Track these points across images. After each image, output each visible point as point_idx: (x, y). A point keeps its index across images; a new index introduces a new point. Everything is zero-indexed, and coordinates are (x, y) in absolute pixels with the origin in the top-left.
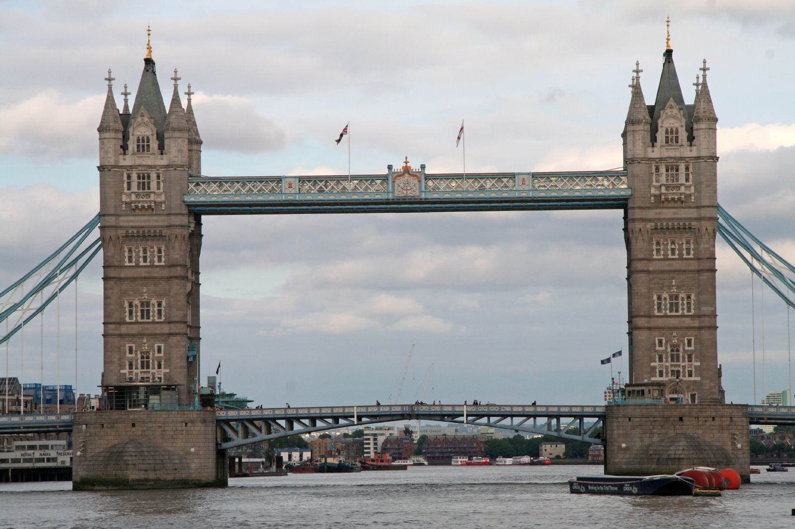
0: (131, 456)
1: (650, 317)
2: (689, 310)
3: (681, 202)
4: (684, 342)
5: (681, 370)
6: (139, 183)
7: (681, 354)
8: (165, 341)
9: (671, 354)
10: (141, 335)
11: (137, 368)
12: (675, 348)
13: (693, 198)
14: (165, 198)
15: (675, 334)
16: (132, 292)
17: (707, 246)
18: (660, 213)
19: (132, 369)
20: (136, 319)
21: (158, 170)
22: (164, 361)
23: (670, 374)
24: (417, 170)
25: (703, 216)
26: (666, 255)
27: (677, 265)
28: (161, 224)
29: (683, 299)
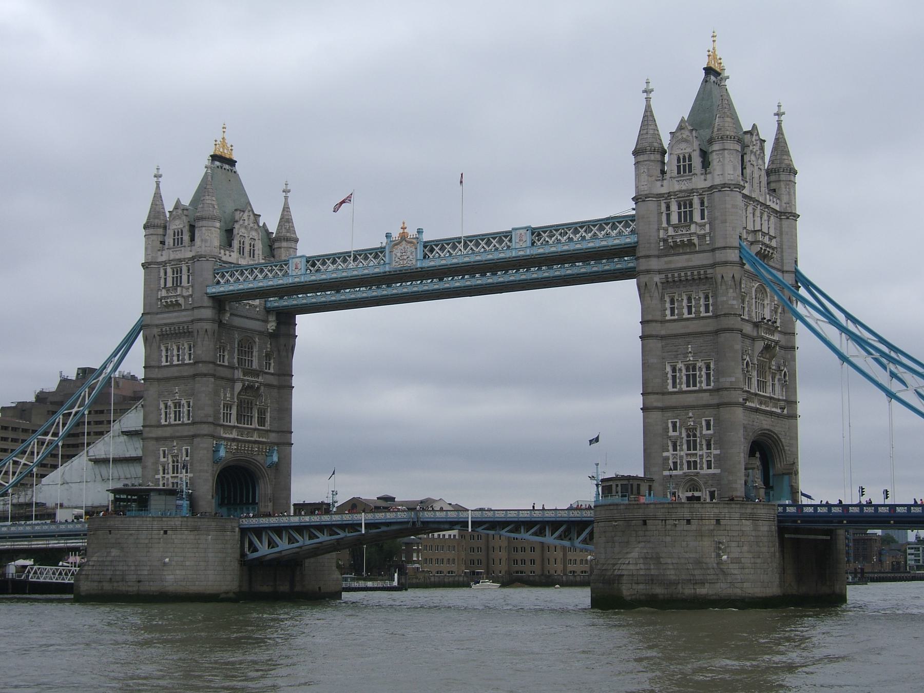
0: (89, 565)
1: (663, 394)
3: (687, 247)
5: (698, 461)
6: (173, 278)
7: (698, 440)
8: (191, 444)
9: (687, 440)
10: (172, 438)
11: (168, 473)
12: (691, 432)
13: (708, 238)
14: (192, 292)
18: (670, 262)
21: (187, 263)
23: (685, 466)
24: (415, 236)
25: (718, 260)
27: (694, 327)
28: (185, 319)
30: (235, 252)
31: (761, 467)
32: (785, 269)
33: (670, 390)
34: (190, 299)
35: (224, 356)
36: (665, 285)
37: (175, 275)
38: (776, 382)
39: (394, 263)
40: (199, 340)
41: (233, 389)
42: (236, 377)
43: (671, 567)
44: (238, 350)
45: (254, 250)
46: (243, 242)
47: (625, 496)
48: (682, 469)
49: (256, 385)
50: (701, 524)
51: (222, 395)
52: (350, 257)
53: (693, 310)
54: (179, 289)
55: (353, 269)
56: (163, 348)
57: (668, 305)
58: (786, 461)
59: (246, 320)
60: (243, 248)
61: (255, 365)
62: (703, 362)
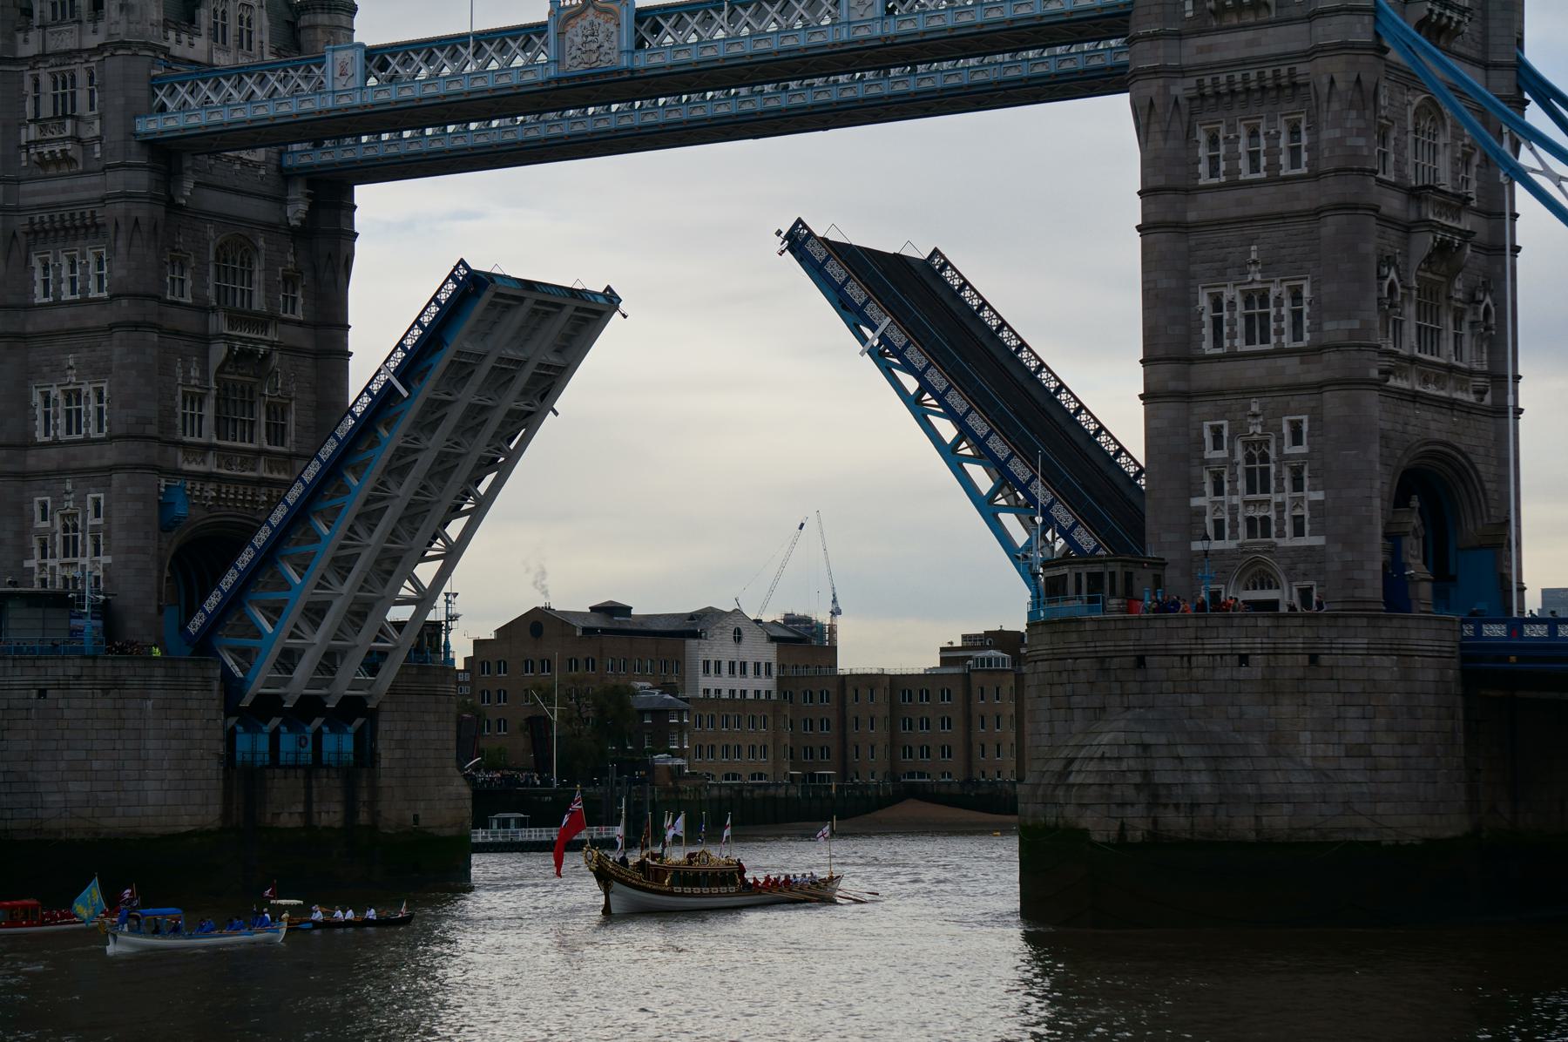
2: (1298, 336)
4: (1281, 430)
5: (1273, 515)
6: (55, 96)
8: (106, 487)
9: (1248, 470)
10: (61, 473)
11: (53, 556)
12: (1257, 452)
14: (101, 129)
15: (1255, 408)
16: (46, 369)
17: (1337, 133)
18: (1210, 48)
19: (46, 558)
20: (55, 433)
21: (87, 61)
22: (105, 537)
23: (1242, 530)
26: (1233, 171)
27: (1263, 201)
29: (1279, 302)
30: (205, 36)
31: (1421, 532)
32: (1495, 58)
33: (1207, 352)
34: (97, 148)
35: (182, 281)
36: (1197, 103)
37: (60, 91)
38: (1466, 330)
39: (568, 61)
40: (120, 243)
41: (205, 357)
42: (212, 329)
43: (1201, 765)
44: (218, 267)
45: (250, 33)
46: (224, 12)
47: (1096, 600)
48: (1234, 535)
49: (262, 349)
50: (1272, 664)
51: (179, 372)
52: (466, 46)
53: (1263, 161)
54: (68, 123)
55: (473, 74)
56: (36, 262)
57: (1203, 152)
58: (1489, 516)
59: (234, 198)
60: (224, 27)
61: (259, 303)
62: (1285, 284)
